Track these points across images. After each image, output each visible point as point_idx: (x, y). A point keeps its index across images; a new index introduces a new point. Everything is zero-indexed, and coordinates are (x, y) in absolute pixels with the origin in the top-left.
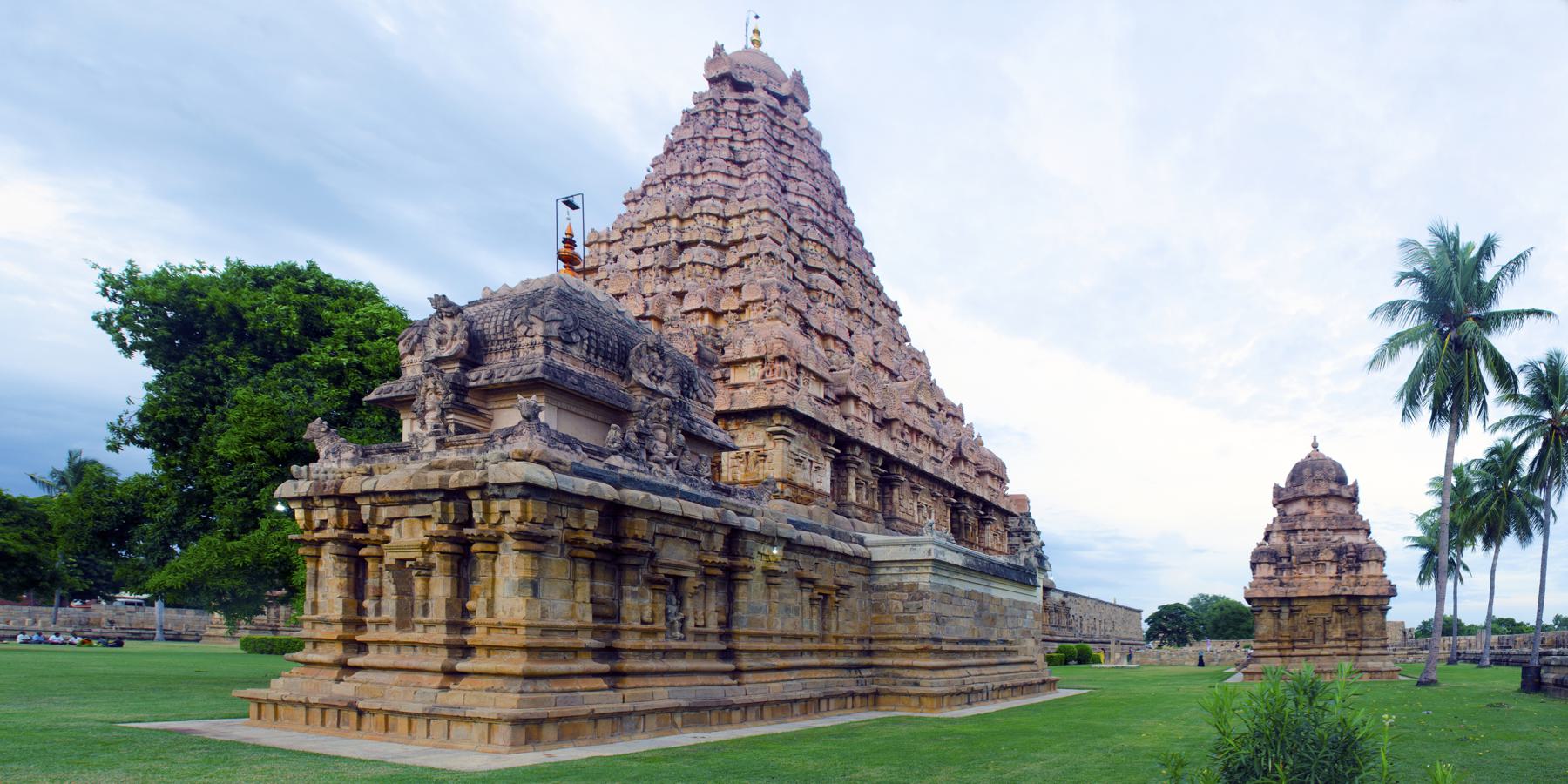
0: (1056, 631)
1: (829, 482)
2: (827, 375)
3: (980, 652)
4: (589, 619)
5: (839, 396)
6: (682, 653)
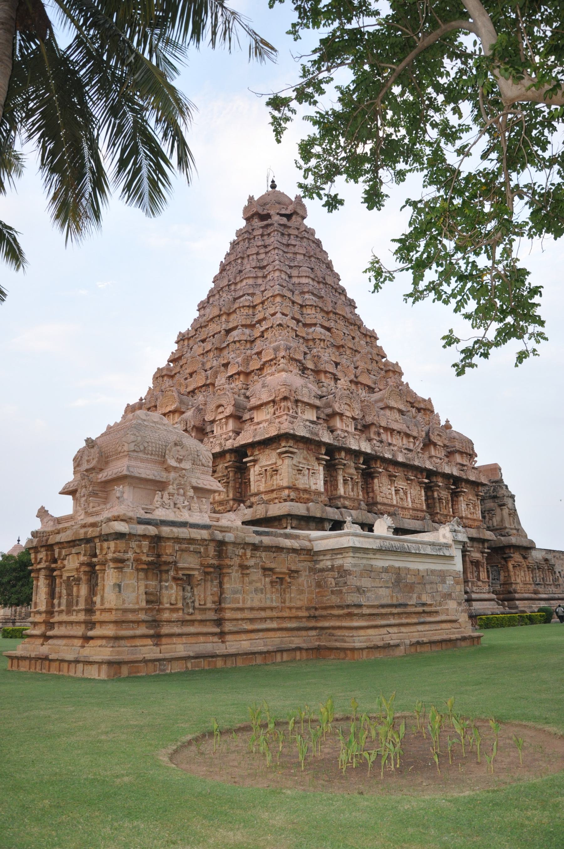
1: (322, 482)
2: (318, 403)
3: (398, 614)
4: (144, 604)
5: (328, 415)
6: (192, 622)
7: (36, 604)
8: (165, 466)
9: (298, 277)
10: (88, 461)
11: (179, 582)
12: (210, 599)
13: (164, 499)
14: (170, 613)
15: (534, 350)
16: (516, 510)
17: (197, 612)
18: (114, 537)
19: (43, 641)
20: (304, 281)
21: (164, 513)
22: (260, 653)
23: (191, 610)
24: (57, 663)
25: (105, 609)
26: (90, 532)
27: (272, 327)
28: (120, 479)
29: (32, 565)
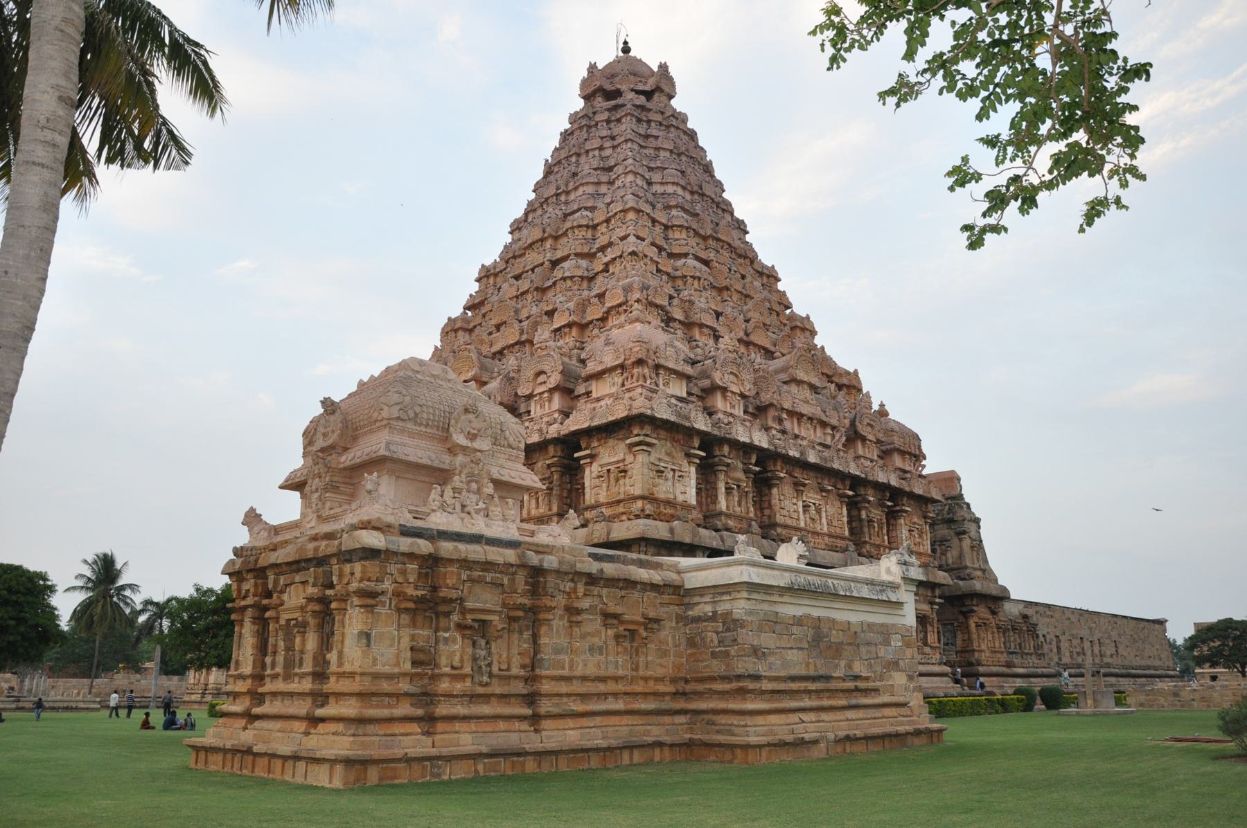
0: (1016, 660)
2: (688, 370)
3: (817, 691)
4: (407, 666)
5: (703, 390)
6: (486, 698)
7: (237, 662)
8: (448, 446)
9: (662, 183)
10: (325, 435)
11: (467, 632)
12: (516, 661)
13: (446, 497)
14: (450, 682)
15: (1118, 201)
16: (981, 541)
17: (495, 681)
18: (361, 555)
19: (246, 725)
20: (670, 189)
21: (444, 520)
22: (597, 750)
23: (485, 679)
24: (266, 760)
25: (344, 673)
26: (322, 547)
27: (621, 257)
28: (375, 463)
29: (233, 601)
